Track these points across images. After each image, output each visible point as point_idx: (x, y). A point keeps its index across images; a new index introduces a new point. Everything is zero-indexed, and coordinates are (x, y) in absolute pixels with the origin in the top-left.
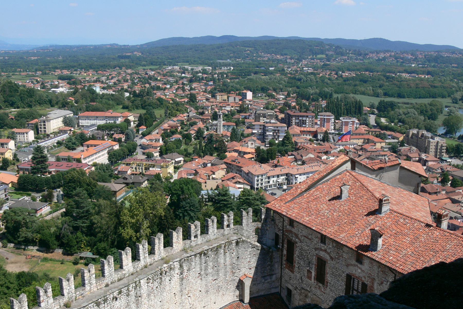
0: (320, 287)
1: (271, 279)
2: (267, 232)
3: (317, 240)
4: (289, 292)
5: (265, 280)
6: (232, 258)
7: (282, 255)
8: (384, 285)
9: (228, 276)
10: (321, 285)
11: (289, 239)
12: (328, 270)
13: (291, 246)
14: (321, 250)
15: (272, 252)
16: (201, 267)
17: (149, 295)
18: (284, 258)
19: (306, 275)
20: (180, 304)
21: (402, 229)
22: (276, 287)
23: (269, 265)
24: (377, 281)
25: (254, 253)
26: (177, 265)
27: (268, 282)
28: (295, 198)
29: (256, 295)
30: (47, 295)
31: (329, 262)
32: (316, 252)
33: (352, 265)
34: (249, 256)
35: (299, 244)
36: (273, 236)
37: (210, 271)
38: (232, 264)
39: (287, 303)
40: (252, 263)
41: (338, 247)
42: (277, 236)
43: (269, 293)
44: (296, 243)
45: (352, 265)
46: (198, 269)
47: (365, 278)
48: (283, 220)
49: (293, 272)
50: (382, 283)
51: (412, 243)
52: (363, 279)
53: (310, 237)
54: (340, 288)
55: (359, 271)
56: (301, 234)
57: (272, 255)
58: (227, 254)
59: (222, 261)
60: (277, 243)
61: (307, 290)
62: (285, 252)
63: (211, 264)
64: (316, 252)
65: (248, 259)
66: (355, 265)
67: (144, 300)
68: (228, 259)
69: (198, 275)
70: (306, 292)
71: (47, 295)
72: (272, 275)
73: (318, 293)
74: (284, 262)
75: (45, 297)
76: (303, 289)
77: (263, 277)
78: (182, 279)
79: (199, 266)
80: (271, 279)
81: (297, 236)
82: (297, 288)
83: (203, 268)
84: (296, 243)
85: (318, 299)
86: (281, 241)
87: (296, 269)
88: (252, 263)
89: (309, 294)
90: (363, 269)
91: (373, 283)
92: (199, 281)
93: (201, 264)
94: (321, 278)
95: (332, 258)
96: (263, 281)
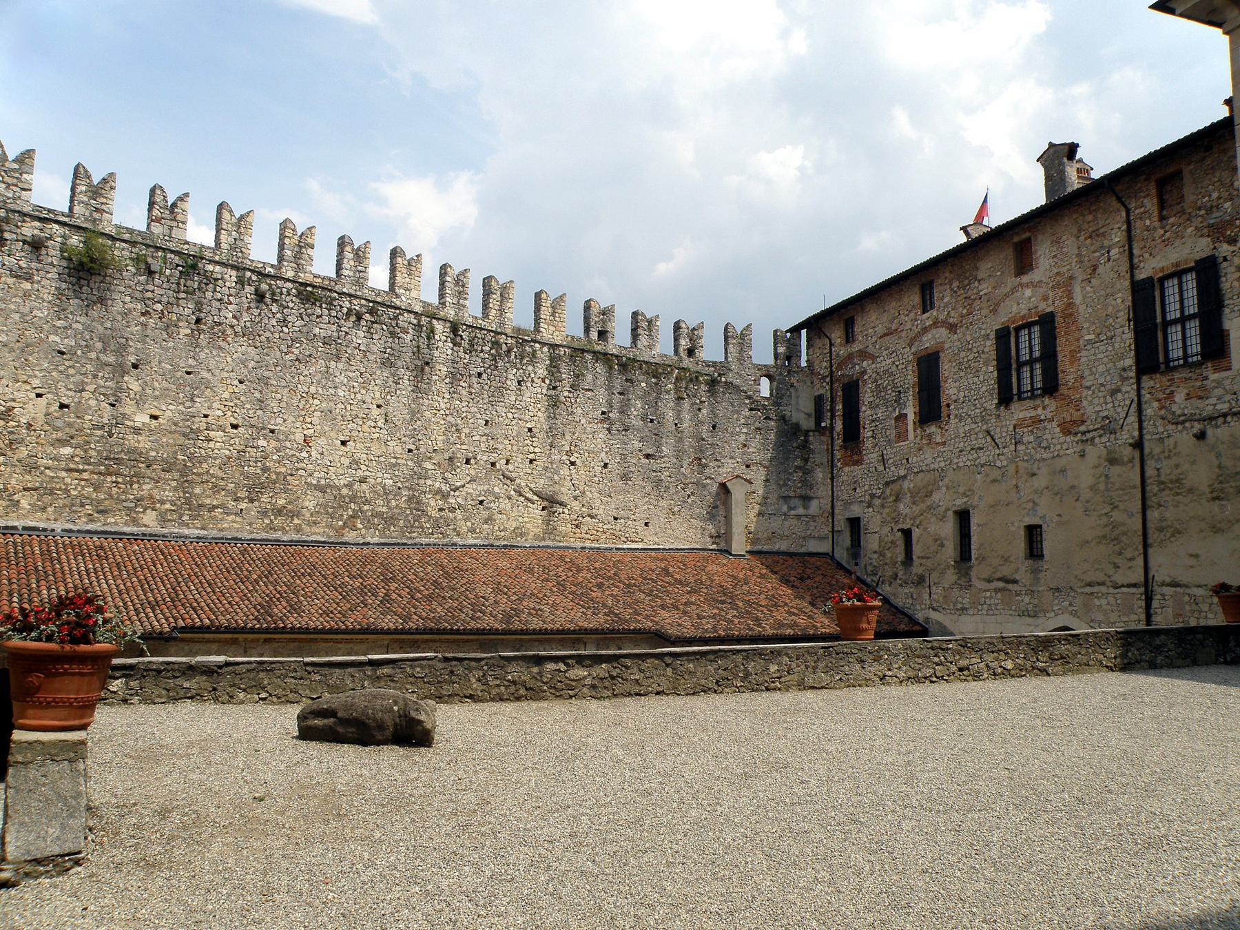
5: (791, 509)
7: (832, 439)
8: (1100, 270)
9: (685, 463)
17: (455, 377)
18: (839, 442)
22: (821, 538)
25: (757, 425)
27: (799, 517)
32: (913, 349)
34: (745, 430)
40: (751, 450)
41: (966, 282)
42: (819, 400)
43: (803, 550)
48: (831, 345)
50: (1095, 268)
57: (806, 441)
58: (686, 403)
60: (819, 418)
62: (839, 426)
64: (913, 349)
65: (743, 437)
68: (686, 416)
74: (838, 455)
77: (786, 498)
78: (554, 403)
80: (806, 507)
83: (617, 406)
87: (869, 444)
88: (751, 450)
91: (1069, 294)
92: (602, 435)
95: (952, 328)
96: (785, 508)
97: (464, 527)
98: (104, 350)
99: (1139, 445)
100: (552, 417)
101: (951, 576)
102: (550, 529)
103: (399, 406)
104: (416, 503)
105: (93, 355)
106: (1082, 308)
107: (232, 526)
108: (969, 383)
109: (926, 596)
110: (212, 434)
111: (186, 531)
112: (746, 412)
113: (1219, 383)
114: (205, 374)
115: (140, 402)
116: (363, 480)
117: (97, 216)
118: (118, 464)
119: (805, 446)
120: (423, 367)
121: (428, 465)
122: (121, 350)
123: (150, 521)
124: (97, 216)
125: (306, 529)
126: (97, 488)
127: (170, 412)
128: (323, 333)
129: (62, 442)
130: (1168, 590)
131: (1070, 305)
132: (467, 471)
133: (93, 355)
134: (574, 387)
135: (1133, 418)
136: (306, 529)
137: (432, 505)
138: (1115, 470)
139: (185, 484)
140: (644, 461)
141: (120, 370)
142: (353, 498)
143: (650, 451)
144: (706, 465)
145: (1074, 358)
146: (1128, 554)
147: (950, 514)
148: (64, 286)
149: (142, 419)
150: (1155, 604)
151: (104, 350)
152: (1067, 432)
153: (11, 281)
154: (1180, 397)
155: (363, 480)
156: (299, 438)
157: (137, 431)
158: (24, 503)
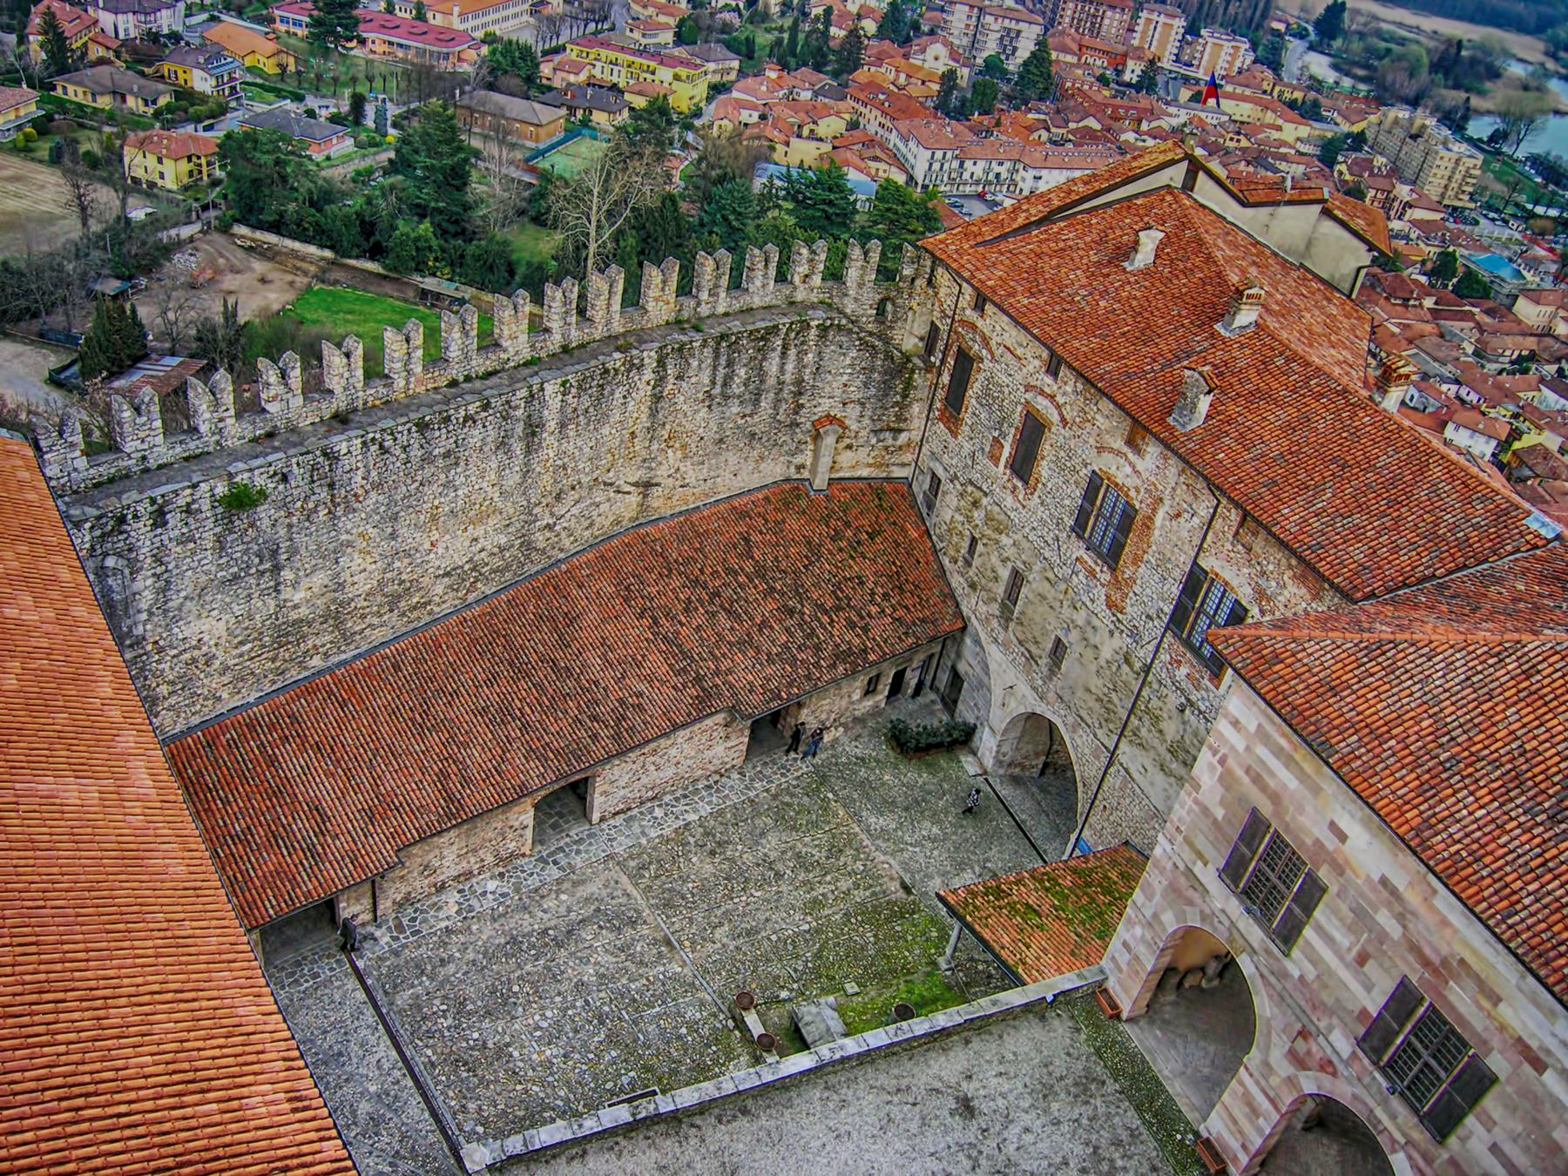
0: (1015, 487)
1: (895, 439)
2: (910, 314)
3: (1037, 363)
4: (936, 482)
6: (801, 365)
8: (1181, 520)
10: (1019, 484)
11: (964, 346)
12: (1046, 448)
13: (965, 364)
14: (1042, 393)
15: (913, 372)
16: (714, 375)
17: (563, 426)
18: (941, 394)
19: (987, 449)
20: (644, 461)
21: (1275, 385)
22: (904, 465)
23: (897, 403)
24: (1166, 508)
26: (650, 357)
28: (1004, 237)
29: (848, 475)
30: (286, 385)
31: (1054, 429)
33: (1112, 450)
35: (987, 364)
36: (923, 330)
37: (737, 388)
38: (799, 382)
39: (924, 511)
42: (934, 329)
44: (981, 360)
45: (1112, 450)
46: (706, 381)
47: (1138, 491)
49: (955, 434)
50: (1178, 515)
51: (1289, 428)
52: (1132, 493)
53: (1019, 352)
54: (1067, 502)
55: (1128, 470)
56: (999, 340)
57: (910, 378)
59: (772, 366)
60: (930, 350)
61: (980, 489)
62: (946, 379)
63: (742, 372)
65: (846, 377)
66: (1119, 453)
67: (548, 438)
68: (790, 367)
69: (700, 395)
70: (978, 494)
71: (286, 385)
72: (900, 431)
73: (1009, 501)
74: (938, 405)
75: (281, 389)
76: (971, 483)
78: (657, 398)
79: (708, 372)
81: (986, 341)
82: (957, 477)
84: (981, 360)
85: (1002, 517)
86: (940, 345)
89: (985, 501)
90: (1138, 468)
91: (1154, 510)
92: (703, 413)
93: (715, 368)
94: (1023, 466)
95: (1063, 420)
96: (874, 441)
97: (567, 543)
98: (261, 562)
99: (1147, 669)
100: (653, 413)
101: (995, 608)
102: (643, 507)
103: (512, 479)
104: (528, 546)
105: (253, 571)
106: (1157, 532)
107: (378, 636)
108: (1057, 484)
109: (974, 601)
110: (355, 579)
111: (344, 656)
112: (854, 353)
113: (1207, 690)
114: (344, 537)
115: (295, 585)
116: (482, 550)
117: (221, 425)
118: (287, 633)
119: (908, 385)
120: (533, 429)
121: (536, 510)
122: (275, 553)
123: (316, 662)
124: (221, 425)
125: (436, 609)
126: (273, 660)
127: (320, 579)
128: (442, 450)
129: (242, 643)
130: (1123, 772)
131: (1150, 518)
132: (574, 495)
133: (253, 571)
134: (679, 378)
135: (1151, 647)
136: (436, 609)
137: (540, 539)
138: (1125, 668)
139: (339, 625)
140: (740, 422)
141: (277, 568)
142: (473, 569)
143: (748, 411)
144: (802, 406)
145: (1137, 560)
146: (1111, 726)
147: (1010, 565)
148: (218, 530)
149: (299, 596)
150: (1112, 770)
151: (261, 562)
152: (1109, 607)
153: (178, 549)
154: (1183, 671)
155: (482, 550)
156: (427, 546)
157: (296, 607)
158: (225, 695)
